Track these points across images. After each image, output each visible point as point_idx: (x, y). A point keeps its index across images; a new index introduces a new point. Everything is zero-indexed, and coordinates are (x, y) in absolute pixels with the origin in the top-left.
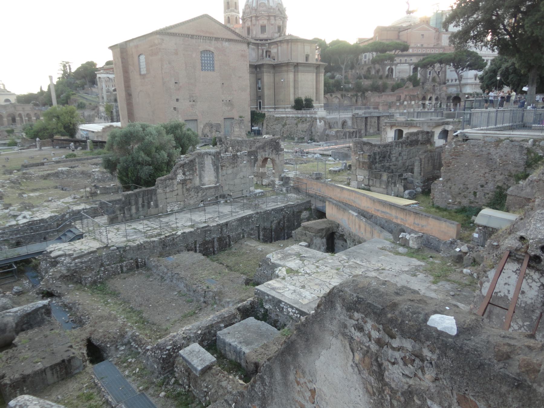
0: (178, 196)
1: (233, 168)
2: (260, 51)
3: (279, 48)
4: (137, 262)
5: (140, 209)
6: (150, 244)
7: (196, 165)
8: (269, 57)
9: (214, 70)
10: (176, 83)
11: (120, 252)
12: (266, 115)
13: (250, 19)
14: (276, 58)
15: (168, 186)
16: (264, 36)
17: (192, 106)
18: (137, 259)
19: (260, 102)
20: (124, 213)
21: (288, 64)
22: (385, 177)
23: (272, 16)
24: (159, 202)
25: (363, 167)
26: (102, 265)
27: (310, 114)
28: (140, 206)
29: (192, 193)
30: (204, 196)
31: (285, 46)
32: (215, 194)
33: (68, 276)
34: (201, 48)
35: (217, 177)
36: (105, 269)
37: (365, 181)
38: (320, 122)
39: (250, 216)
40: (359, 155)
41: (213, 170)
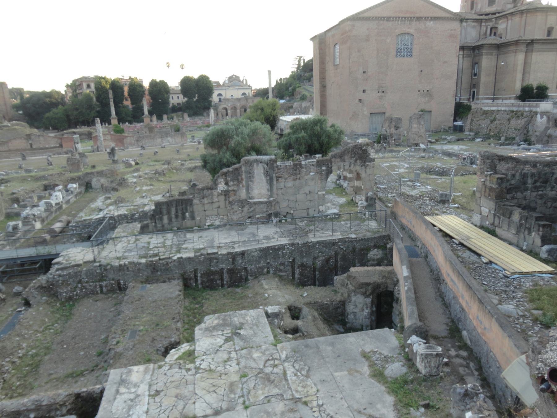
0: (220, 210)
1: (295, 180)
2: (483, 29)
3: (510, 22)
4: (119, 284)
5: (174, 220)
6: (135, 266)
7: (242, 175)
8: (495, 34)
9: (411, 56)
10: (364, 72)
11: (101, 269)
12: (472, 108)
14: (503, 36)
15: (207, 197)
16: (493, 9)
17: (381, 97)
18: (119, 280)
19: (474, 92)
20: (155, 222)
21: (517, 43)
22: (516, 217)
24: (196, 214)
25: (489, 195)
26: (80, 282)
27: (529, 106)
28: (173, 216)
29: (236, 207)
30: (251, 212)
31: (517, 19)
33: (45, 287)
34: (398, 32)
35: (271, 190)
36: (82, 286)
37: (489, 217)
38: (542, 118)
39: (282, 247)
40: (486, 176)
41: (265, 181)
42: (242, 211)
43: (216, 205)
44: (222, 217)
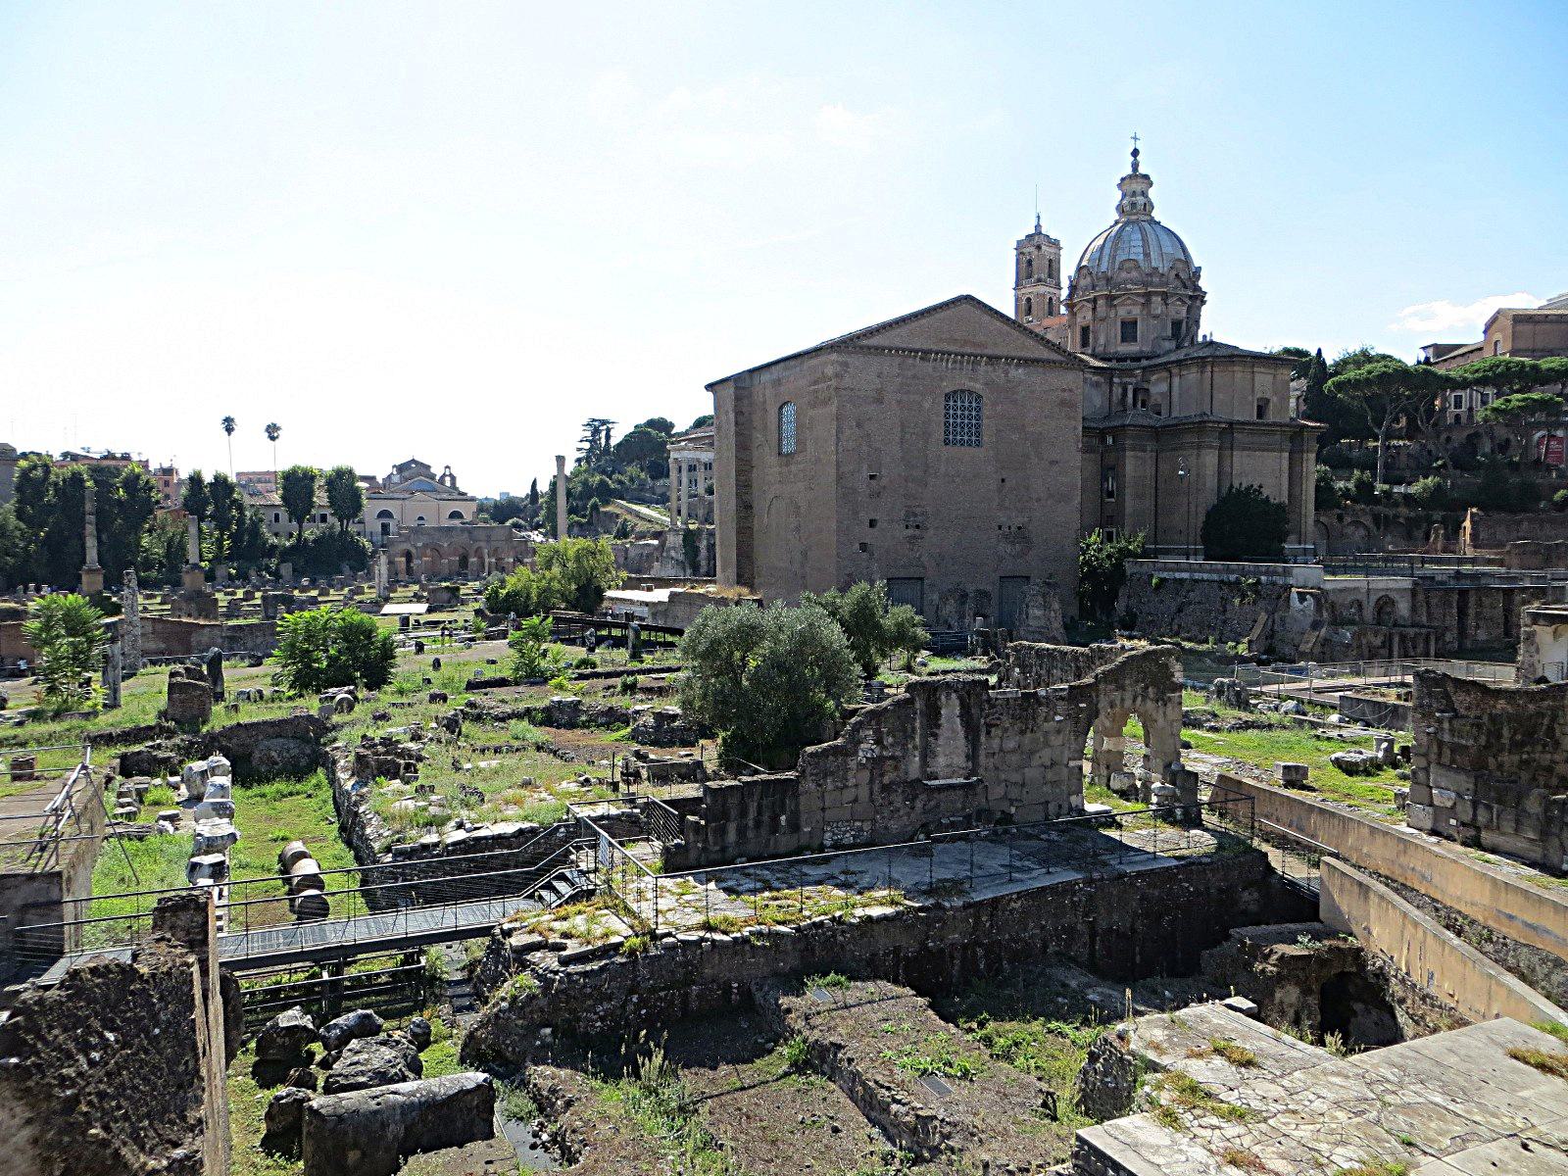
1: (1022, 732)
2: (1117, 391)
8: (1143, 406)
9: (978, 444)
10: (872, 477)
13: (1090, 305)
15: (832, 774)
21: (1200, 426)
23: (1156, 293)
24: (803, 817)
28: (751, 823)
29: (898, 800)
31: (1192, 375)
32: (964, 809)
34: (948, 386)
35: (972, 757)
37: (1459, 808)
39: (1068, 888)
40: (1440, 721)
42: (913, 808)
43: (849, 795)
44: (858, 824)
